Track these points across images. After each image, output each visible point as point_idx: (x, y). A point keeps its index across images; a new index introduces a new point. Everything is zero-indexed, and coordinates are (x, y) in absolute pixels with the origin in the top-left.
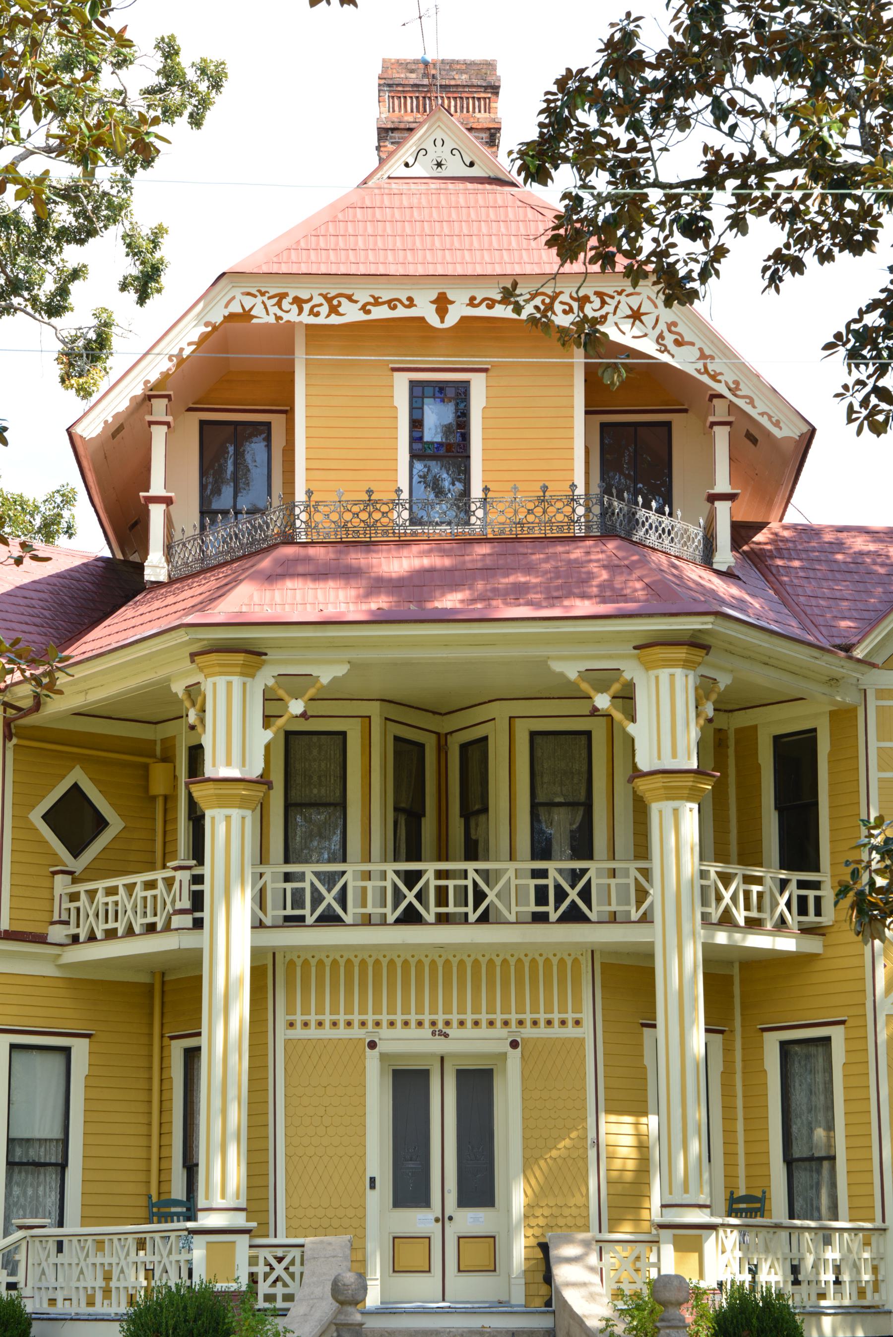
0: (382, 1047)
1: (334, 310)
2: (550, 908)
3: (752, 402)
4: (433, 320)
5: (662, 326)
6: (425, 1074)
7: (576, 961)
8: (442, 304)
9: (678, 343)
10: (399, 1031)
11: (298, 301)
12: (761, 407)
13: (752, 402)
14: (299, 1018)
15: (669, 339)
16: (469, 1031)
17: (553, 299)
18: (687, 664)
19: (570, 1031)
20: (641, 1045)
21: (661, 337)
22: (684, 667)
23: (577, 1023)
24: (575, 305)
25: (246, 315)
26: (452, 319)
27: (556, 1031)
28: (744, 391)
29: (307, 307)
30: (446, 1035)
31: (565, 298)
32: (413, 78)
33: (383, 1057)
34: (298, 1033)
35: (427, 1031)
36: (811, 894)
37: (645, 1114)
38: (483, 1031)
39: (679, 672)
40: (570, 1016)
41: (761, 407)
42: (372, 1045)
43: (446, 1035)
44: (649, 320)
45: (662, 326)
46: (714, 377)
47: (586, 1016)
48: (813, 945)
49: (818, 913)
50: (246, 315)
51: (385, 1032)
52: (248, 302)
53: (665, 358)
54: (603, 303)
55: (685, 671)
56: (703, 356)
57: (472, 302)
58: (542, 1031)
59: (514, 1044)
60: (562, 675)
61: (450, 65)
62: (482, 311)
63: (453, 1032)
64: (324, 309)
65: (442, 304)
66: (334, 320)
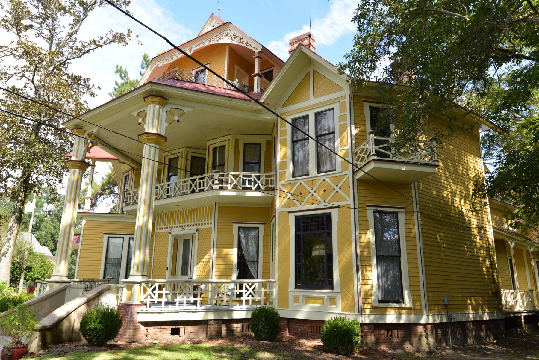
0: (173, 233)
1: (172, 59)
2: (188, 191)
3: (251, 45)
6: (189, 240)
7: (212, 206)
9: (235, 38)
10: (176, 229)
11: (166, 60)
13: (251, 45)
14: (159, 227)
15: (233, 37)
16: (189, 228)
18: (153, 102)
19: (209, 226)
20: (232, 229)
22: (153, 103)
23: (211, 223)
25: (158, 66)
26: (192, 52)
27: (207, 226)
28: (249, 43)
30: (184, 229)
31: (213, 37)
32: (295, 40)
33: (174, 235)
34: (158, 231)
35: (181, 228)
36: (269, 179)
37: (232, 248)
38: (192, 227)
39: (151, 105)
40: (209, 222)
41: (253, 46)
42: (170, 233)
43: (184, 229)
44: (229, 35)
46: (242, 43)
47: (213, 221)
48: (270, 194)
49: (271, 184)
50: (158, 66)
51: (174, 229)
52: (158, 63)
53: (233, 42)
55: (154, 105)
56: (241, 39)
58: (204, 226)
59: (197, 230)
60: (134, 116)
61: (302, 36)
62: (198, 47)
63: (186, 228)
66: (172, 61)
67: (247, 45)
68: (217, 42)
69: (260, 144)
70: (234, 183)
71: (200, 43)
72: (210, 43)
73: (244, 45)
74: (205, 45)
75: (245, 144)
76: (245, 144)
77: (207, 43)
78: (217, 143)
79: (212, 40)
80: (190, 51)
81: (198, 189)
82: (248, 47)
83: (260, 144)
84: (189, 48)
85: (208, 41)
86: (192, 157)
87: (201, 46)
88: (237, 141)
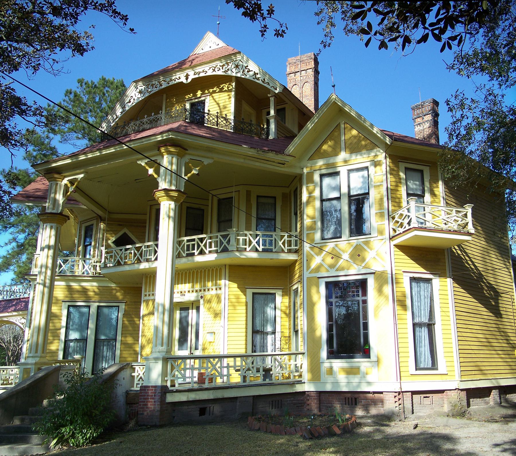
3: (269, 84)
4: (185, 81)
5: (244, 68)
8: (187, 77)
11: (153, 85)
12: (271, 85)
13: (269, 84)
17: (215, 68)
21: (244, 71)
23: (220, 289)
24: (221, 68)
26: (189, 80)
29: (154, 86)
31: (218, 67)
41: (271, 85)
44: (240, 67)
45: (244, 68)
54: (228, 65)
57: (195, 75)
62: (197, 76)
64: (158, 86)
65: (187, 77)
67: (263, 82)
68: (224, 74)
69: (275, 198)
70: (252, 245)
71: (201, 70)
72: (214, 73)
73: (260, 82)
74: (207, 74)
75: (258, 197)
76: (258, 197)
77: (210, 73)
78: (223, 193)
79: (216, 70)
80: (187, 79)
81: (208, 249)
82: (265, 85)
83: (275, 198)
84: (185, 74)
85: (211, 70)
86: (188, 208)
87: (202, 75)
88: (248, 194)
